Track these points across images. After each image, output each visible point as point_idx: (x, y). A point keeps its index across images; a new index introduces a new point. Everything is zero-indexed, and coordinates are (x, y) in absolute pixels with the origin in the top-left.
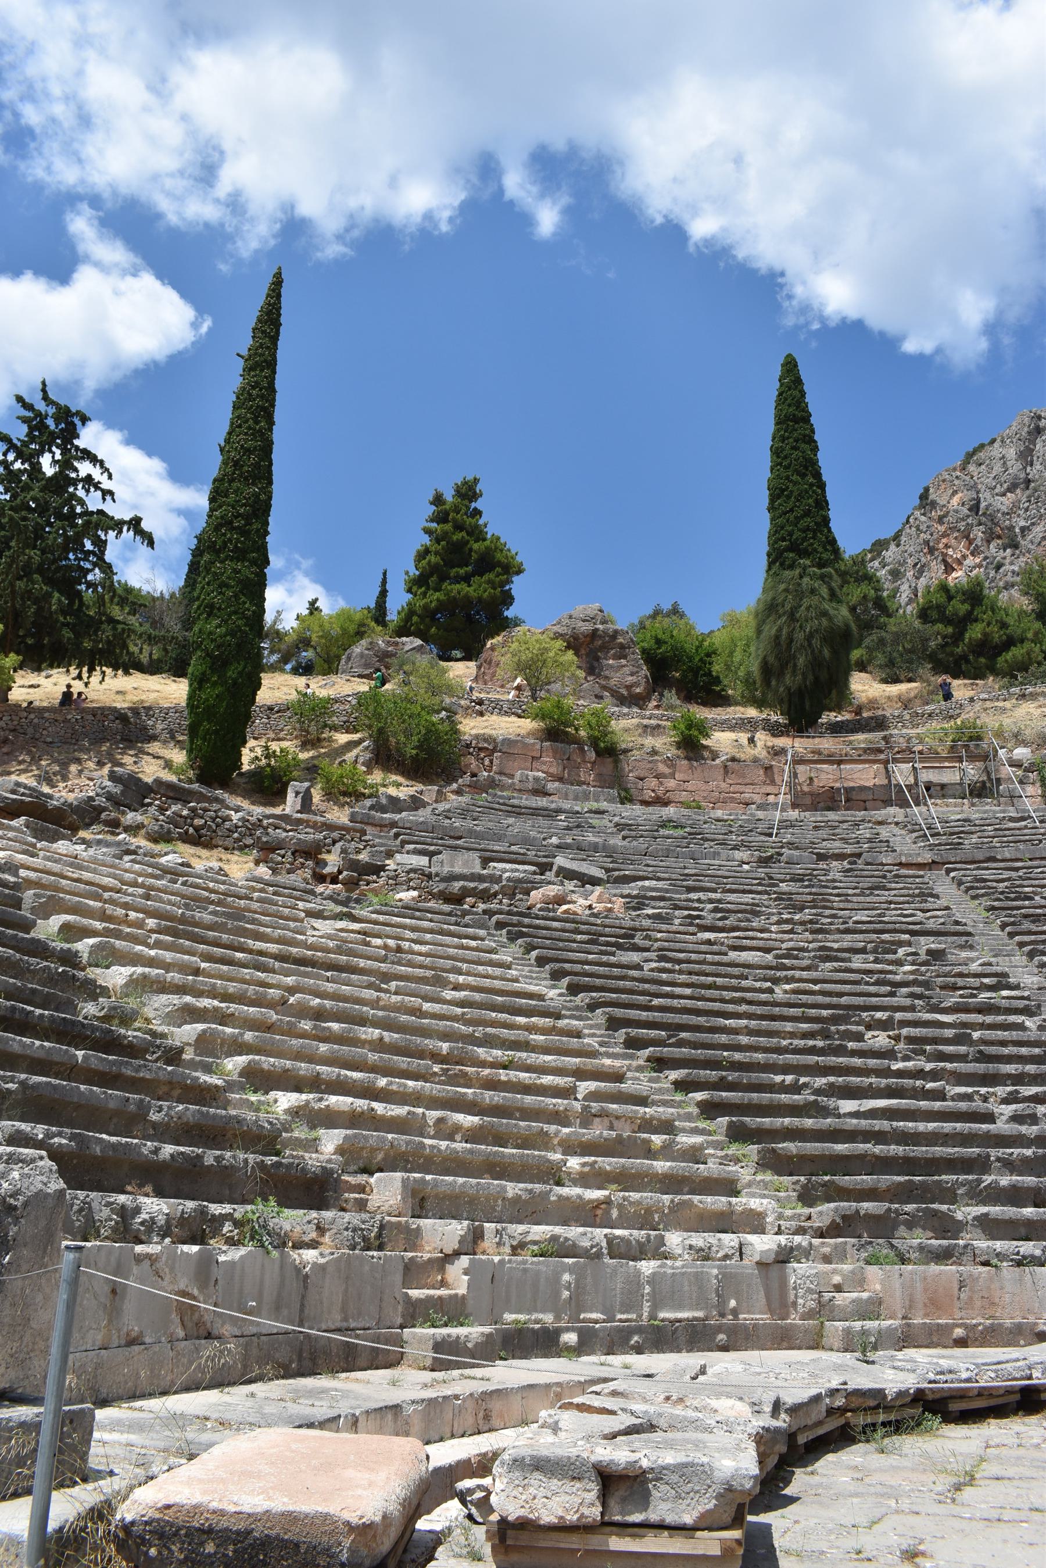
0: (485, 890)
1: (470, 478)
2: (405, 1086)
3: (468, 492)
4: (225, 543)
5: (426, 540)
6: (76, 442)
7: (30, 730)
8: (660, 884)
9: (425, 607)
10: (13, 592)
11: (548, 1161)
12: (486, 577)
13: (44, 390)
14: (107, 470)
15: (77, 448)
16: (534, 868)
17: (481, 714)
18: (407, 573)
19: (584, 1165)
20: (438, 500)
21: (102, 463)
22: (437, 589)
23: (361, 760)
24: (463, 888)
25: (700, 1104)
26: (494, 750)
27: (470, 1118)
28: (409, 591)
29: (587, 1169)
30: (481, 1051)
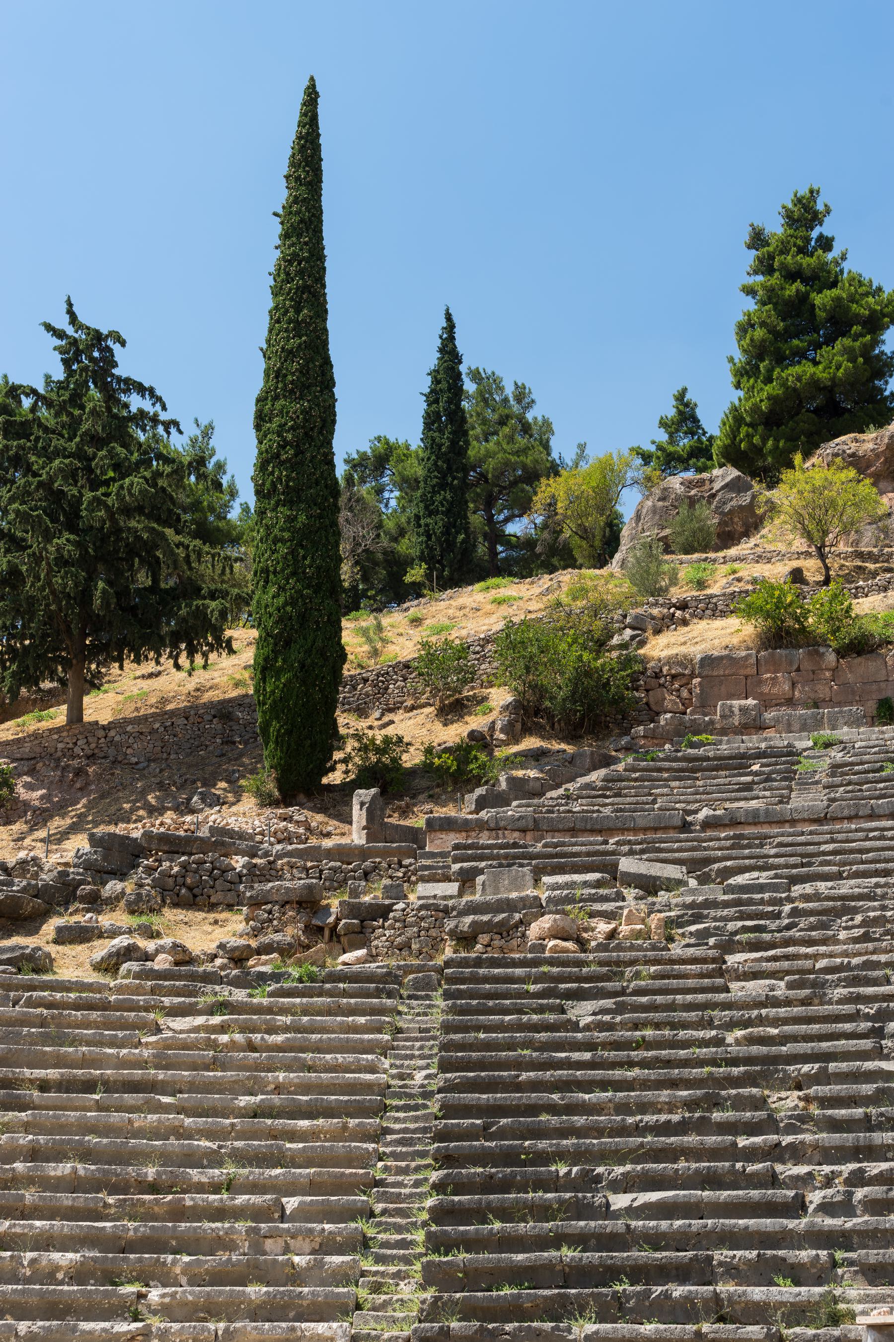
0: (502, 923)
1: (803, 191)
2: (31, 1227)
3: (805, 214)
4: (273, 484)
5: (750, 304)
6: (115, 371)
7: (112, 752)
8: (764, 877)
9: (755, 409)
10: (53, 592)
11: (512, 1262)
12: (838, 345)
13: (71, 313)
14: (159, 399)
15: (119, 379)
16: (597, 876)
17: (685, 622)
18: (731, 360)
19: (163, 1296)
20: (758, 239)
21: (151, 391)
22: (769, 380)
23: (499, 725)
24: (474, 923)
25: (432, 1210)
26: (692, 676)
27: (70, 1255)
28: (738, 386)
29: (167, 1300)
30: (195, 1174)
